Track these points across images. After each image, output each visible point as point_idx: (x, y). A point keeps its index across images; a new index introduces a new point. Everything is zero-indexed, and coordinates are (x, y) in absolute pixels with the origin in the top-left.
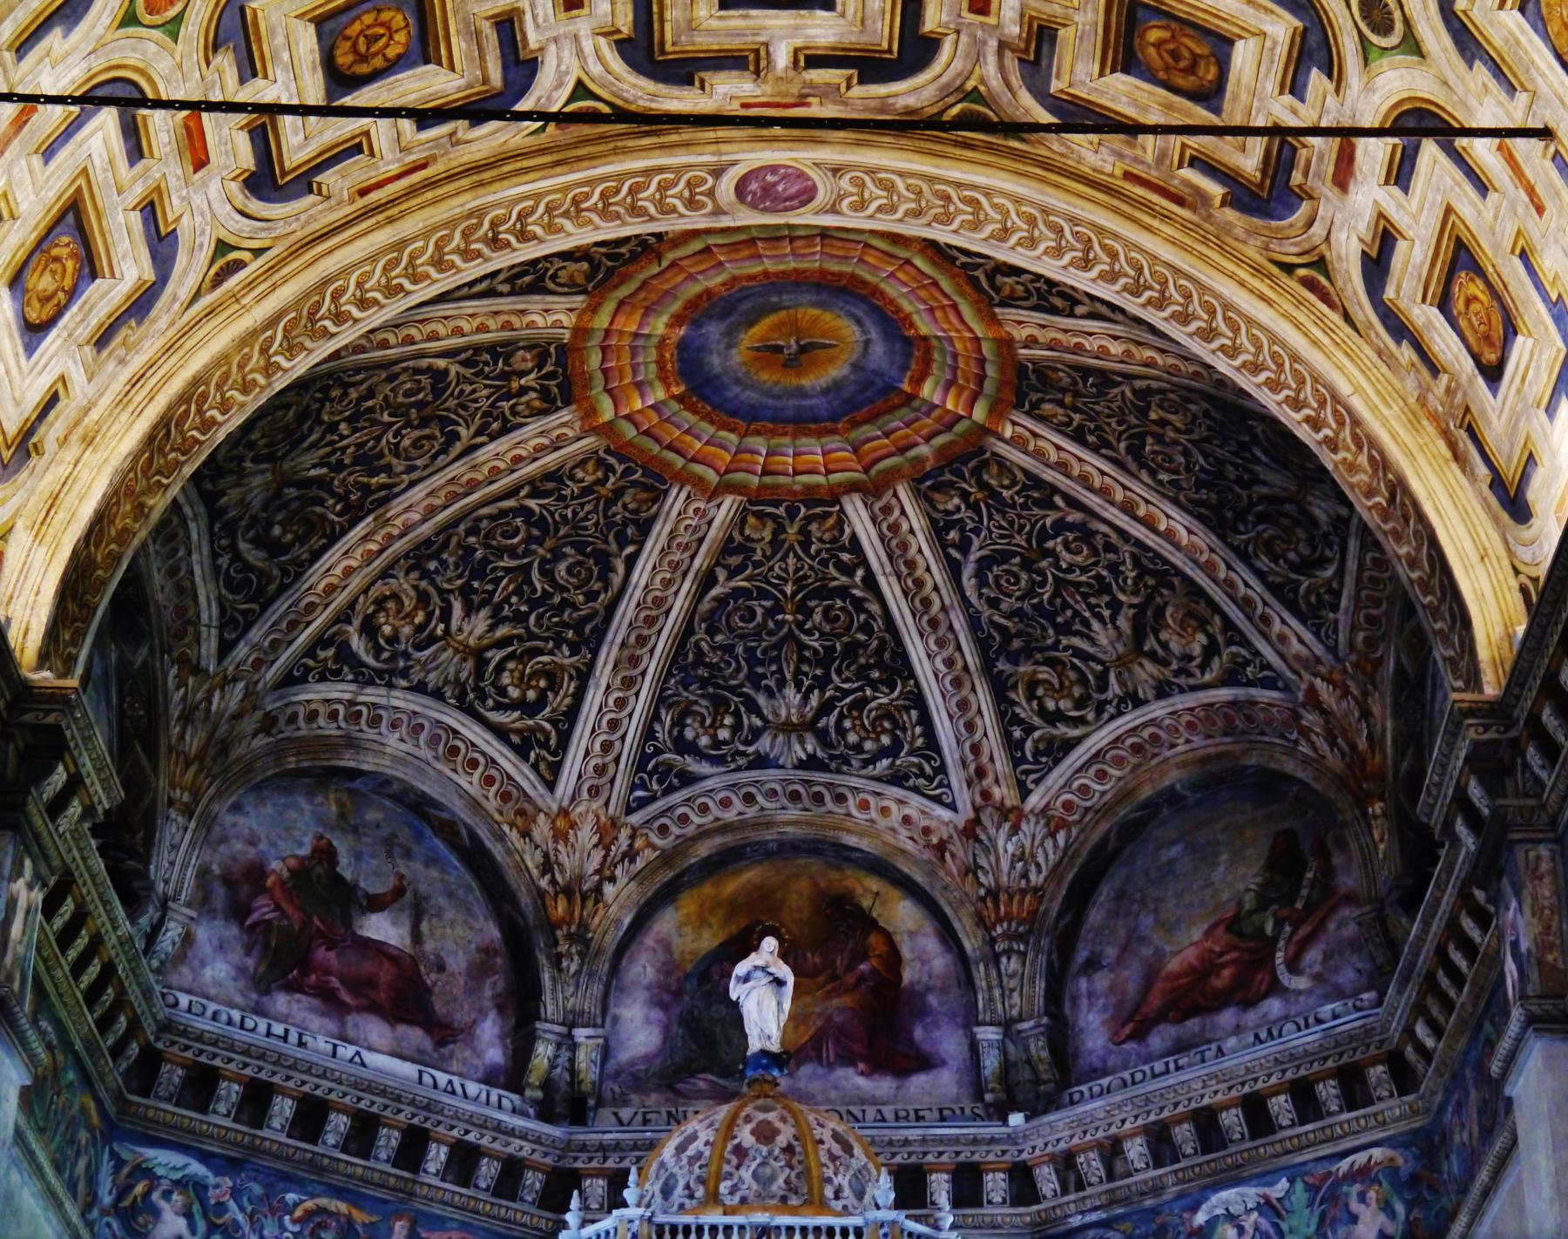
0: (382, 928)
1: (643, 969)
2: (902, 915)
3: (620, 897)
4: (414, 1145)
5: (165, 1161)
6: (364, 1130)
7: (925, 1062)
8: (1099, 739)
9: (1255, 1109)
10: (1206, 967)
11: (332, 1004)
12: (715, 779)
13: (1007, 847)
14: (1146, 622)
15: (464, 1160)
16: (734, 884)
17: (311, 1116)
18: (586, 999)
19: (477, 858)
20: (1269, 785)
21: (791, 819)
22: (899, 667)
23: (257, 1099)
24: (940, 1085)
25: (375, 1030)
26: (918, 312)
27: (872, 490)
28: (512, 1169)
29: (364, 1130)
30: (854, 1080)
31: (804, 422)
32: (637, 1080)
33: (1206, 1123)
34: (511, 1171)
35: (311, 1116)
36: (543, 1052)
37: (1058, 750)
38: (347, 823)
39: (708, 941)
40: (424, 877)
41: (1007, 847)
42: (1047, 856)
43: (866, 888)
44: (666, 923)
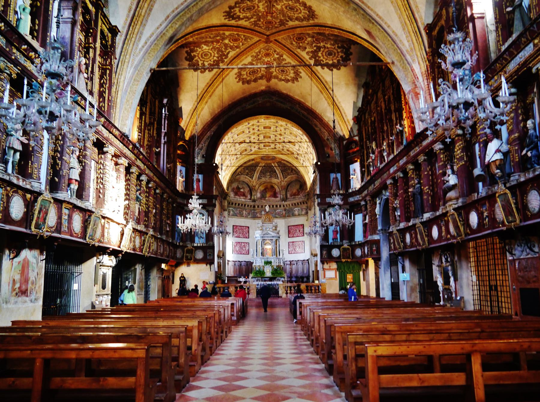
0: (242, 190)
1: (259, 191)
2: (276, 187)
3: (257, 186)
4: (245, 205)
5: (231, 208)
6: (242, 205)
7: (277, 197)
8: (289, 177)
9: (298, 204)
10: (295, 193)
11: (239, 196)
12: (263, 178)
13: (283, 183)
14: (292, 171)
15: (248, 206)
16: (264, 185)
17: (239, 204)
18: (255, 194)
19: (247, 184)
20: (300, 181)
21: (268, 181)
22: (275, 172)
23: (236, 204)
24: (278, 199)
25: (242, 197)
26: (275, 166)
27: (274, 163)
28: (251, 206)
29: (242, 205)
30: (273, 199)
31: (269, 160)
32: (259, 198)
33: (295, 204)
34: (251, 206)
35: (239, 204)
36: (253, 198)
37: (286, 177)
38: (239, 183)
39: (263, 189)
40: (244, 186)
41: (283, 183)
42: (286, 184)
43: (274, 185)
44: (260, 188)
